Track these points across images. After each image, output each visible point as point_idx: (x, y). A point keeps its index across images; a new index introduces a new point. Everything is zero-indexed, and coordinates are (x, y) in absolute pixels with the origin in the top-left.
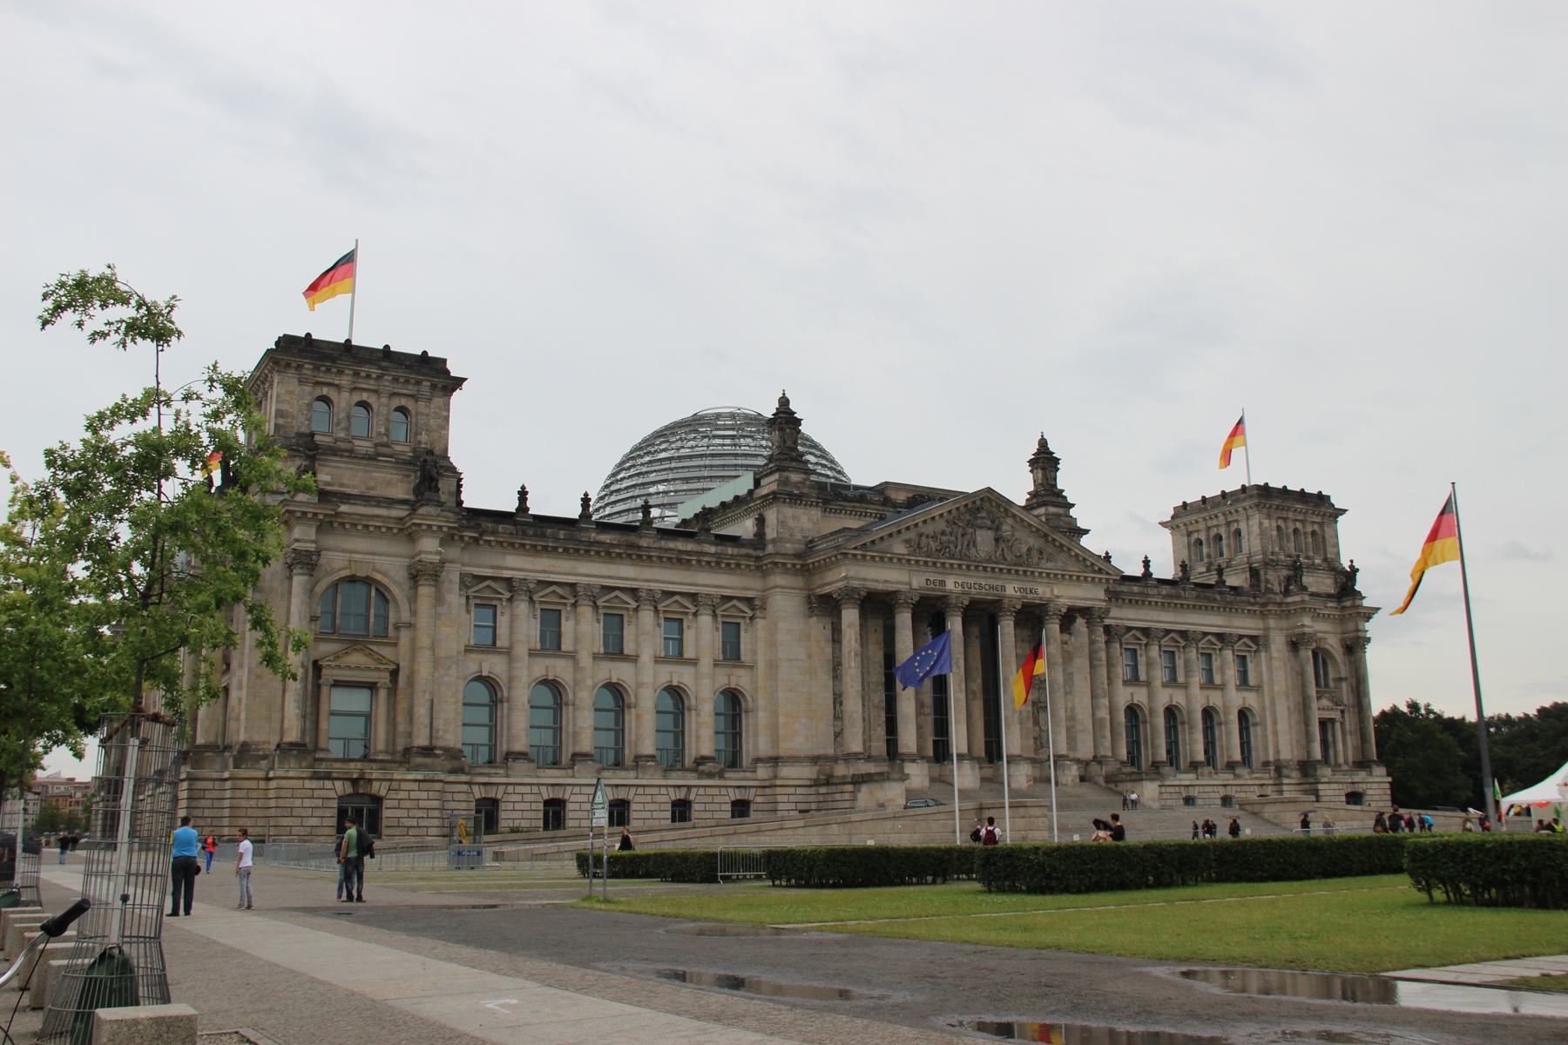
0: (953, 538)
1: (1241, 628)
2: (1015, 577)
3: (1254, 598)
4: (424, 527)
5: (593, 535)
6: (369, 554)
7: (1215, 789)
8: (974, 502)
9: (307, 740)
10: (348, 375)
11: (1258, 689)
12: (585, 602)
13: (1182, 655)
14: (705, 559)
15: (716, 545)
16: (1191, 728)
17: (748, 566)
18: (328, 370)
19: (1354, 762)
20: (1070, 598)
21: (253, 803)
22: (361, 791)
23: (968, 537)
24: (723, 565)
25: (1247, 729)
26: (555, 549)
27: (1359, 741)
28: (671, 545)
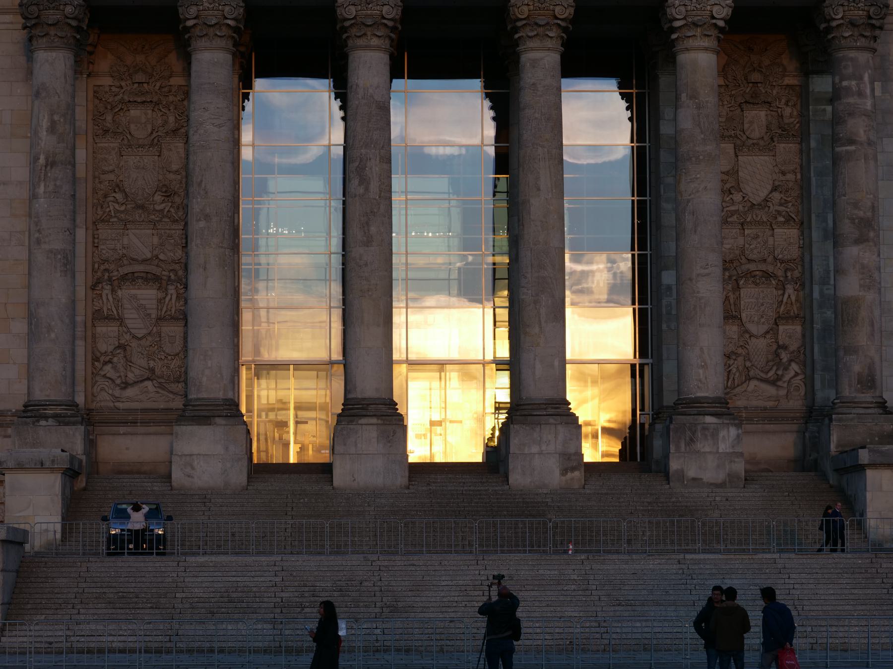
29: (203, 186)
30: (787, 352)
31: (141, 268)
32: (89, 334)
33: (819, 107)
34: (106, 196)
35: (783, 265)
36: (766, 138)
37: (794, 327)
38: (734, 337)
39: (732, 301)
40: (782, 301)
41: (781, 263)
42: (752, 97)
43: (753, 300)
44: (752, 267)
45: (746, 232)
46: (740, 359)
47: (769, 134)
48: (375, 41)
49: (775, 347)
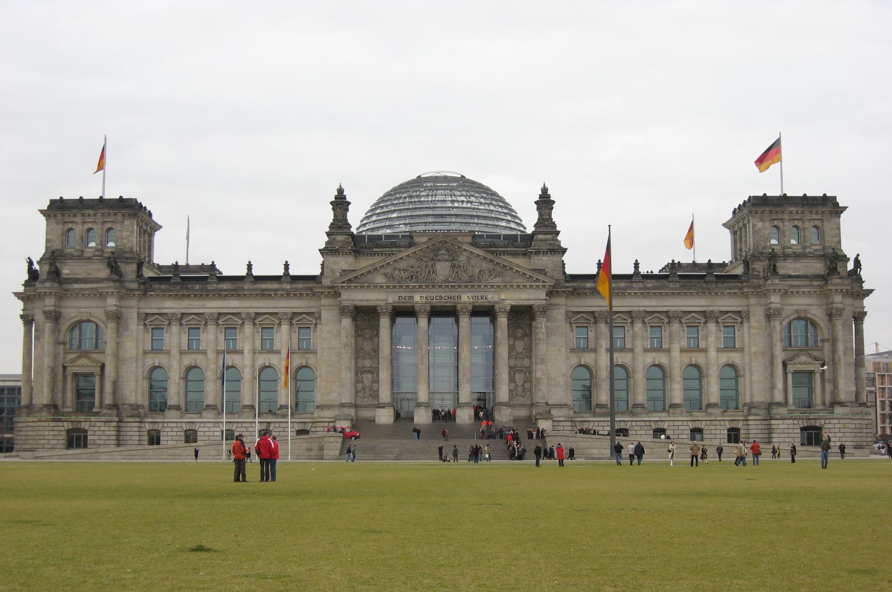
0: (419, 269)
1: (724, 306)
2: (466, 290)
3: (742, 283)
4: (105, 293)
5: (215, 285)
6: (88, 308)
7: (685, 423)
8: (435, 244)
9: (59, 403)
10: (79, 216)
11: (742, 350)
12: (210, 323)
13: (668, 329)
14: (279, 293)
15: (291, 283)
16: (671, 380)
17: (307, 294)
18: (69, 215)
19: (831, 403)
20: (513, 300)
21: (35, 433)
22: (76, 427)
24: (292, 295)
25: (738, 378)
26: (189, 296)
27: (833, 388)
28: (264, 286)
31: (367, 369)
34: (359, 351)
44: (518, 369)
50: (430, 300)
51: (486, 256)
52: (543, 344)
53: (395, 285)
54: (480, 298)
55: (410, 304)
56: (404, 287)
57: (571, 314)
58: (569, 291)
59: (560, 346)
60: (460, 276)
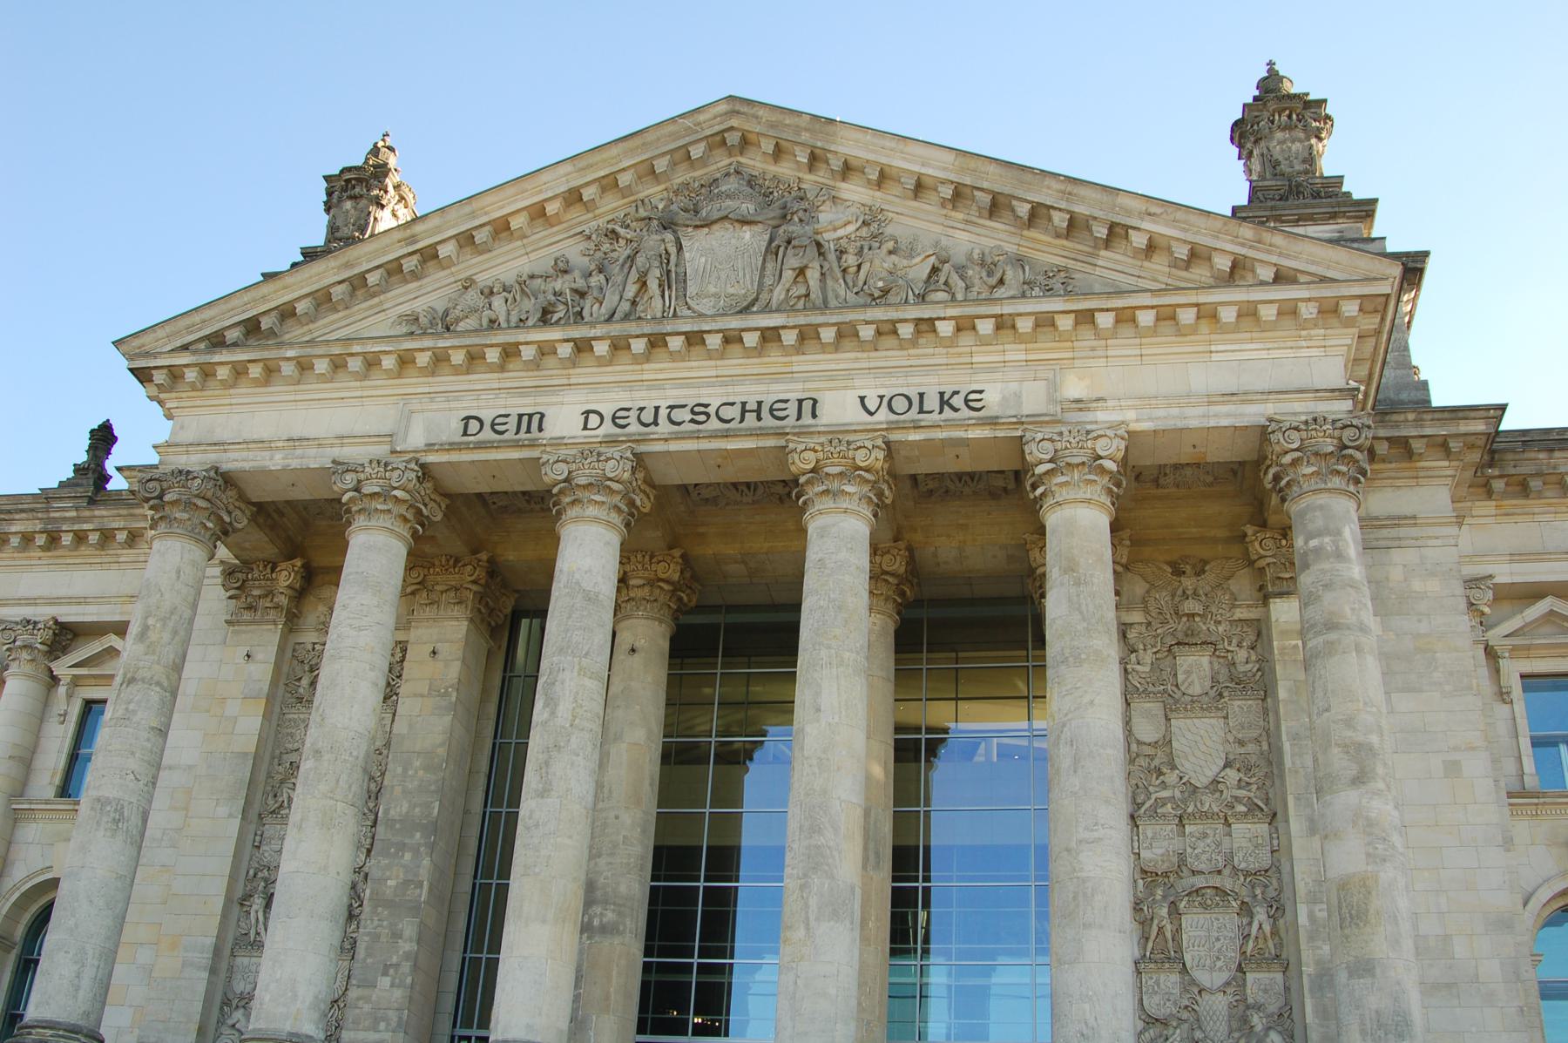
0: (597, 279)
2: (846, 359)
23: (640, 260)
24: (67, 539)
29: (321, 710)
30: (1261, 1014)
32: (224, 966)
33: (1287, 643)
34: (282, 782)
35: (1248, 880)
36: (1212, 693)
37: (1271, 975)
38: (1174, 992)
39: (1169, 935)
40: (1249, 935)
41: (1245, 877)
42: (1187, 635)
43: (1203, 933)
44: (1199, 881)
45: (1188, 829)
46: (1185, 1026)
47: (1215, 689)
48: (592, 511)
49: (1241, 1007)
50: (634, 428)
51: (968, 181)
52: (1358, 649)
53: (441, 343)
54: (932, 403)
55: (516, 454)
56: (493, 356)
57: (1490, 594)
58: (1469, 440)
59: (1456, 749)
60: (816, 294)
